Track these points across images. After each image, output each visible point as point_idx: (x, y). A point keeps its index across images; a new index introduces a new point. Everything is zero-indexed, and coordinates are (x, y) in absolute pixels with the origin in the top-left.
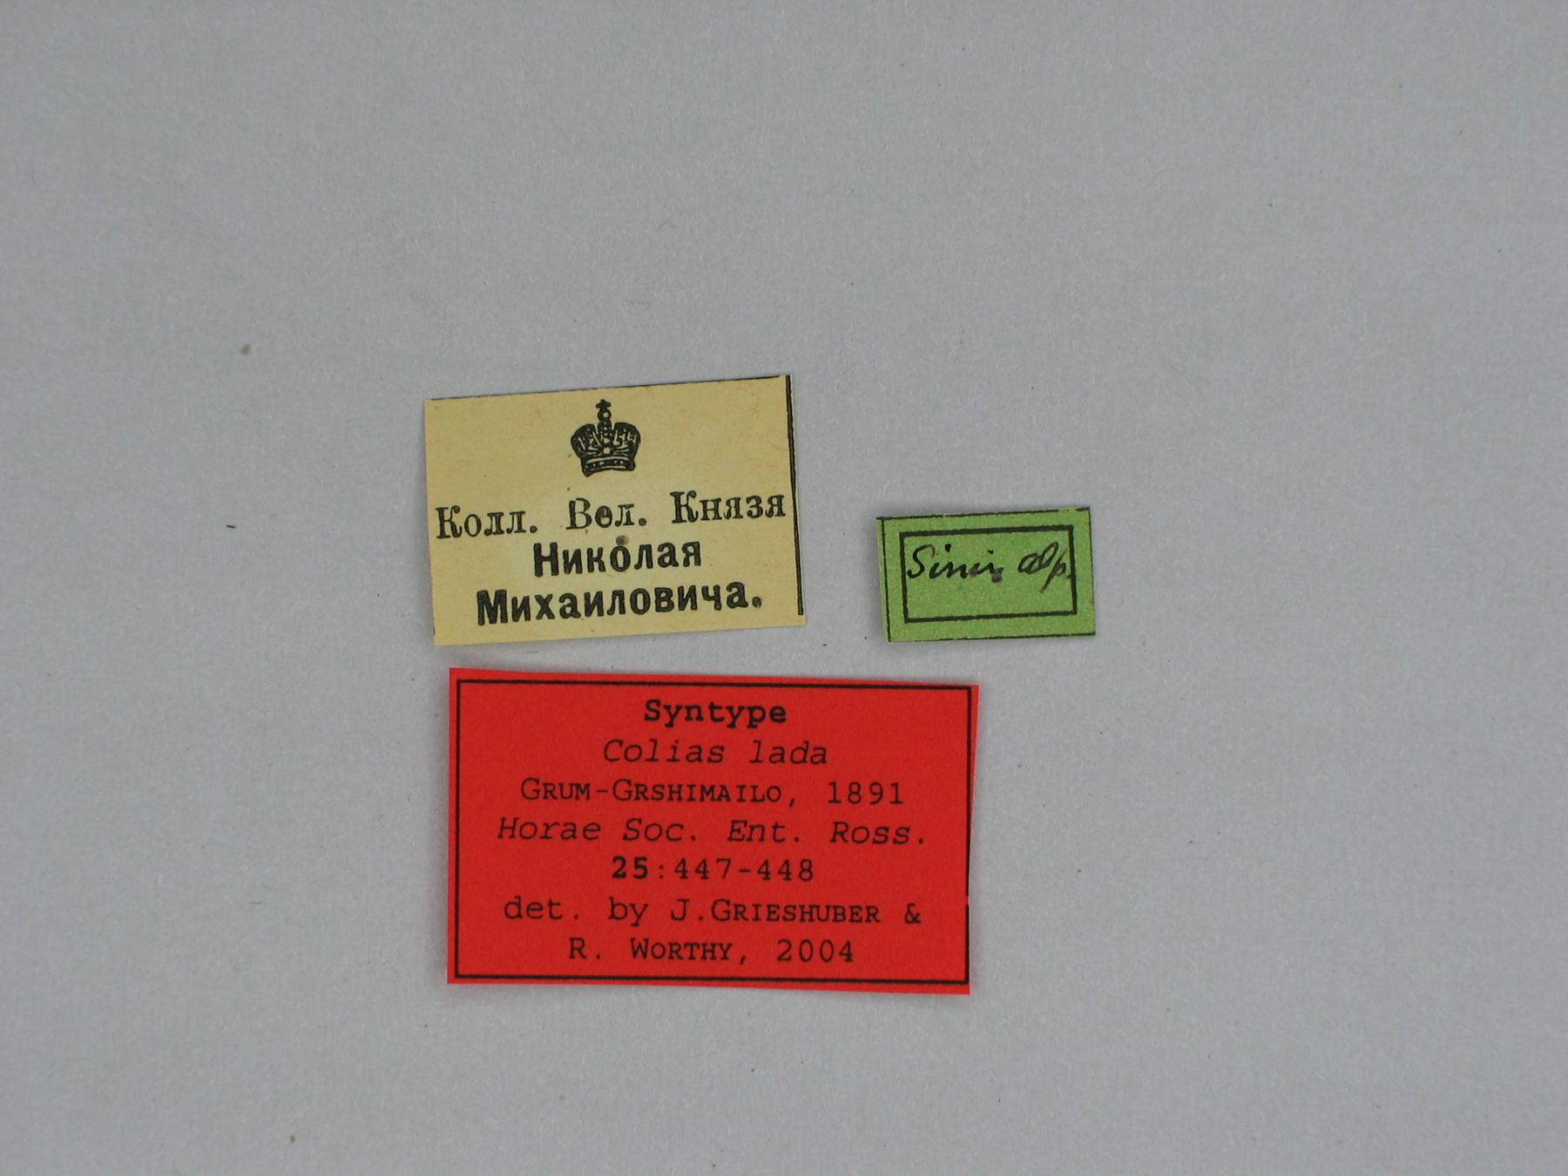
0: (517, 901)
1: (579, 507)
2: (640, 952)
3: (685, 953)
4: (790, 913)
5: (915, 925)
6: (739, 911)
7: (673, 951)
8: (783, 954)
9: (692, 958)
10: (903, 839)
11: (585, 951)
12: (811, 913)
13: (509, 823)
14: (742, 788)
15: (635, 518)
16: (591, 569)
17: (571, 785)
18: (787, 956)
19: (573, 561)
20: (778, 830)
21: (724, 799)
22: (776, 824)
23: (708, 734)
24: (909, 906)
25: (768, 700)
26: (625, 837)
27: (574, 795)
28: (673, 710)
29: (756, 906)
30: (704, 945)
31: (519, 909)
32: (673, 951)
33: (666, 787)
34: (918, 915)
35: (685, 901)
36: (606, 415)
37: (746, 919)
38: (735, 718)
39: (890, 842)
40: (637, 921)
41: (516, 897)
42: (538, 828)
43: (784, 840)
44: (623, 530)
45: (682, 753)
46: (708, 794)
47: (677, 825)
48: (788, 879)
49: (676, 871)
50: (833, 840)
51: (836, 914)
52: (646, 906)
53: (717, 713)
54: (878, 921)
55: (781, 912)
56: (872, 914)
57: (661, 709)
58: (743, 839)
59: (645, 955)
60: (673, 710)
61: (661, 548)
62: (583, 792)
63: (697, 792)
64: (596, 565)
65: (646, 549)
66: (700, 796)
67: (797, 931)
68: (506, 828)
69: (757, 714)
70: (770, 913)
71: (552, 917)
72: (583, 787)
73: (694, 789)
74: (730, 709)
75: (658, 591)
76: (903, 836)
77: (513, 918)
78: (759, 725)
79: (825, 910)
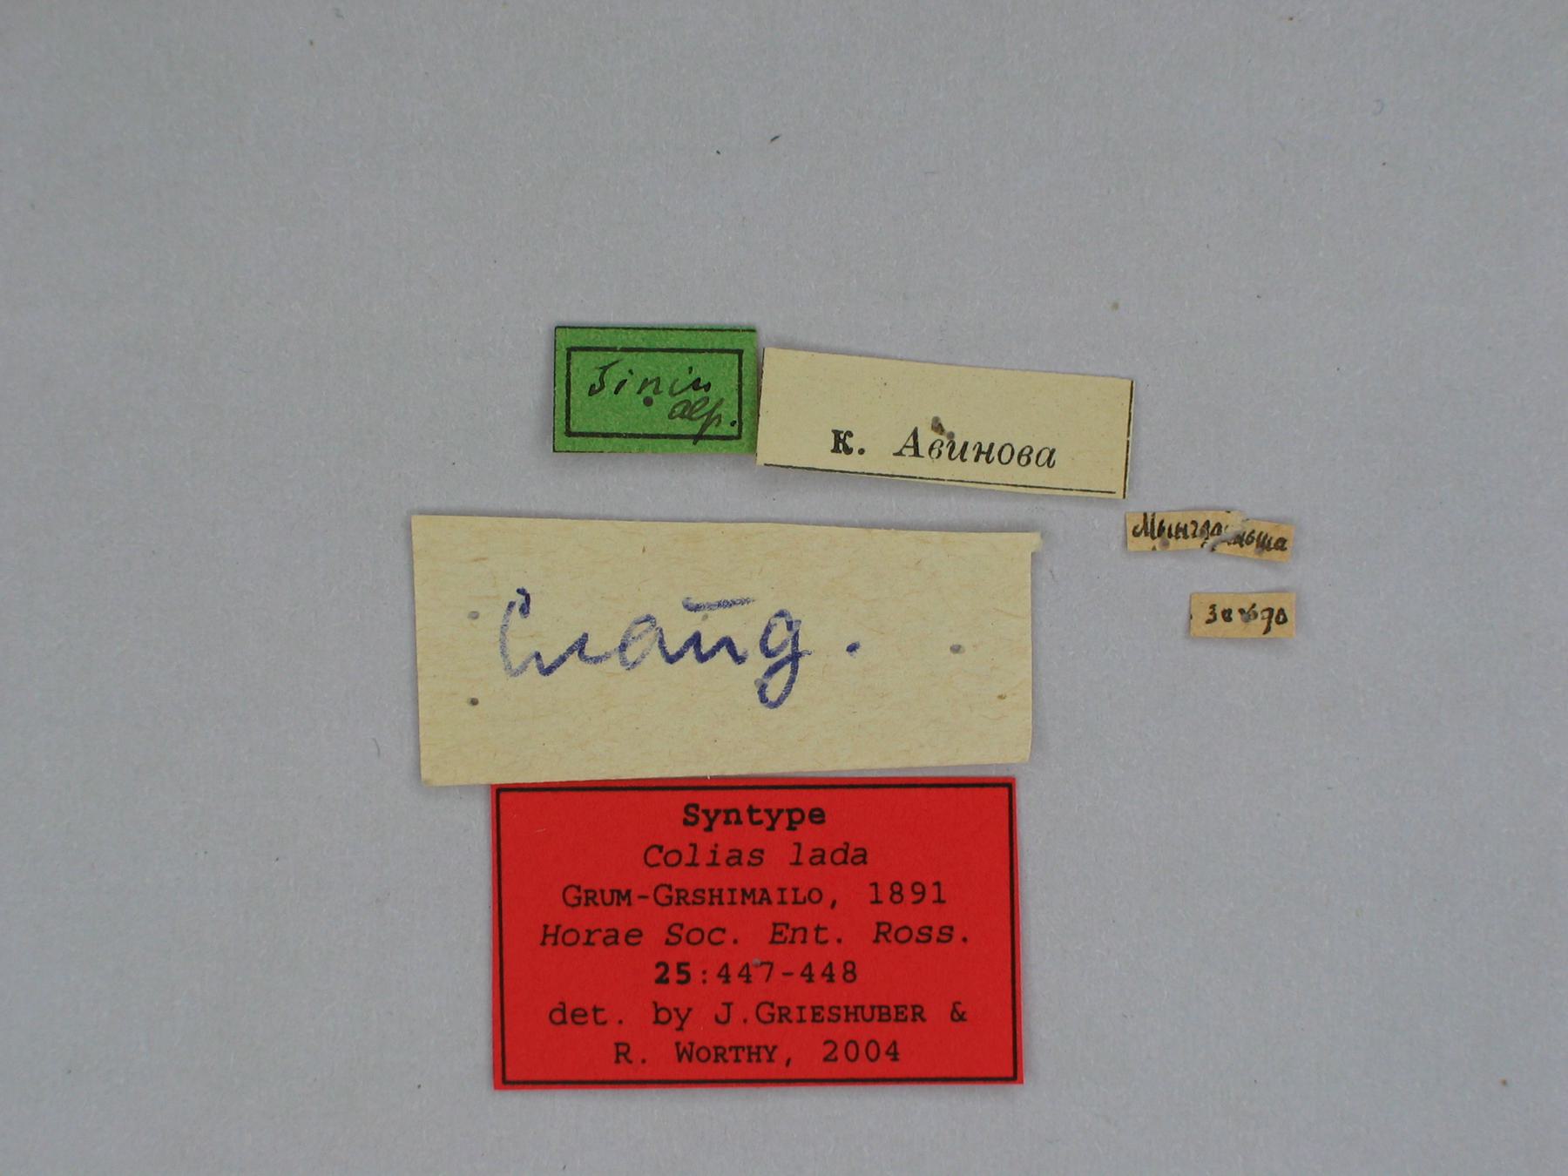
0: (561, 1007)
2: (685, 1055)
3: (730, 1055)
4: (833, 1014)
5: (961, 1022)
6: (784, 1015)
7: (719, 1054)
8: (830, 1055)
9: (737, 1060)
11: (630, 1056)
12: (856, 1014)
13: (551, 930)
14: (782, 890)
17: (612, 891)
18: (833, 1057)
20: (820, 932)
21: (765, 902)
23: (748, 837)
24: (954, 1004)
25: (806, 801)
26: (667, 942)
28: (712, 814)
29: (801, 1008)
31: (567, 1015)
32: (719, 1054)
34: (963, 1013)
37: (790, 1022)
38: (774, 821)
40: (682, 1024)
41: (561, 1003)
42: (581, 936)
43: (826, 942)
45: (722, 856)
46: (749, 898)
47: (718, 929)
48: (831, 980)
49: (719, 975)
50: (876, 941)
51: (881, 1014)
52: (689, 1010)
53: (756, 817)
54: (923, 1020)
55: (825, 1014)
56: (918, 1014)
57: (700, 814)
58: (784, 942)
59: (690, 1059)
60: (712, 814)
62: (624, 899)
63: (738, 897)
67: (842, 1031)
68: (550, 935)
69: (797, 816)
70: (814, 1014)
71: (597, 1023)
72: (624, 893)
73: (735, 893)
74: (769, 811)
77: (559, 1024)
78: (799, 827)
79: (870, 1010)
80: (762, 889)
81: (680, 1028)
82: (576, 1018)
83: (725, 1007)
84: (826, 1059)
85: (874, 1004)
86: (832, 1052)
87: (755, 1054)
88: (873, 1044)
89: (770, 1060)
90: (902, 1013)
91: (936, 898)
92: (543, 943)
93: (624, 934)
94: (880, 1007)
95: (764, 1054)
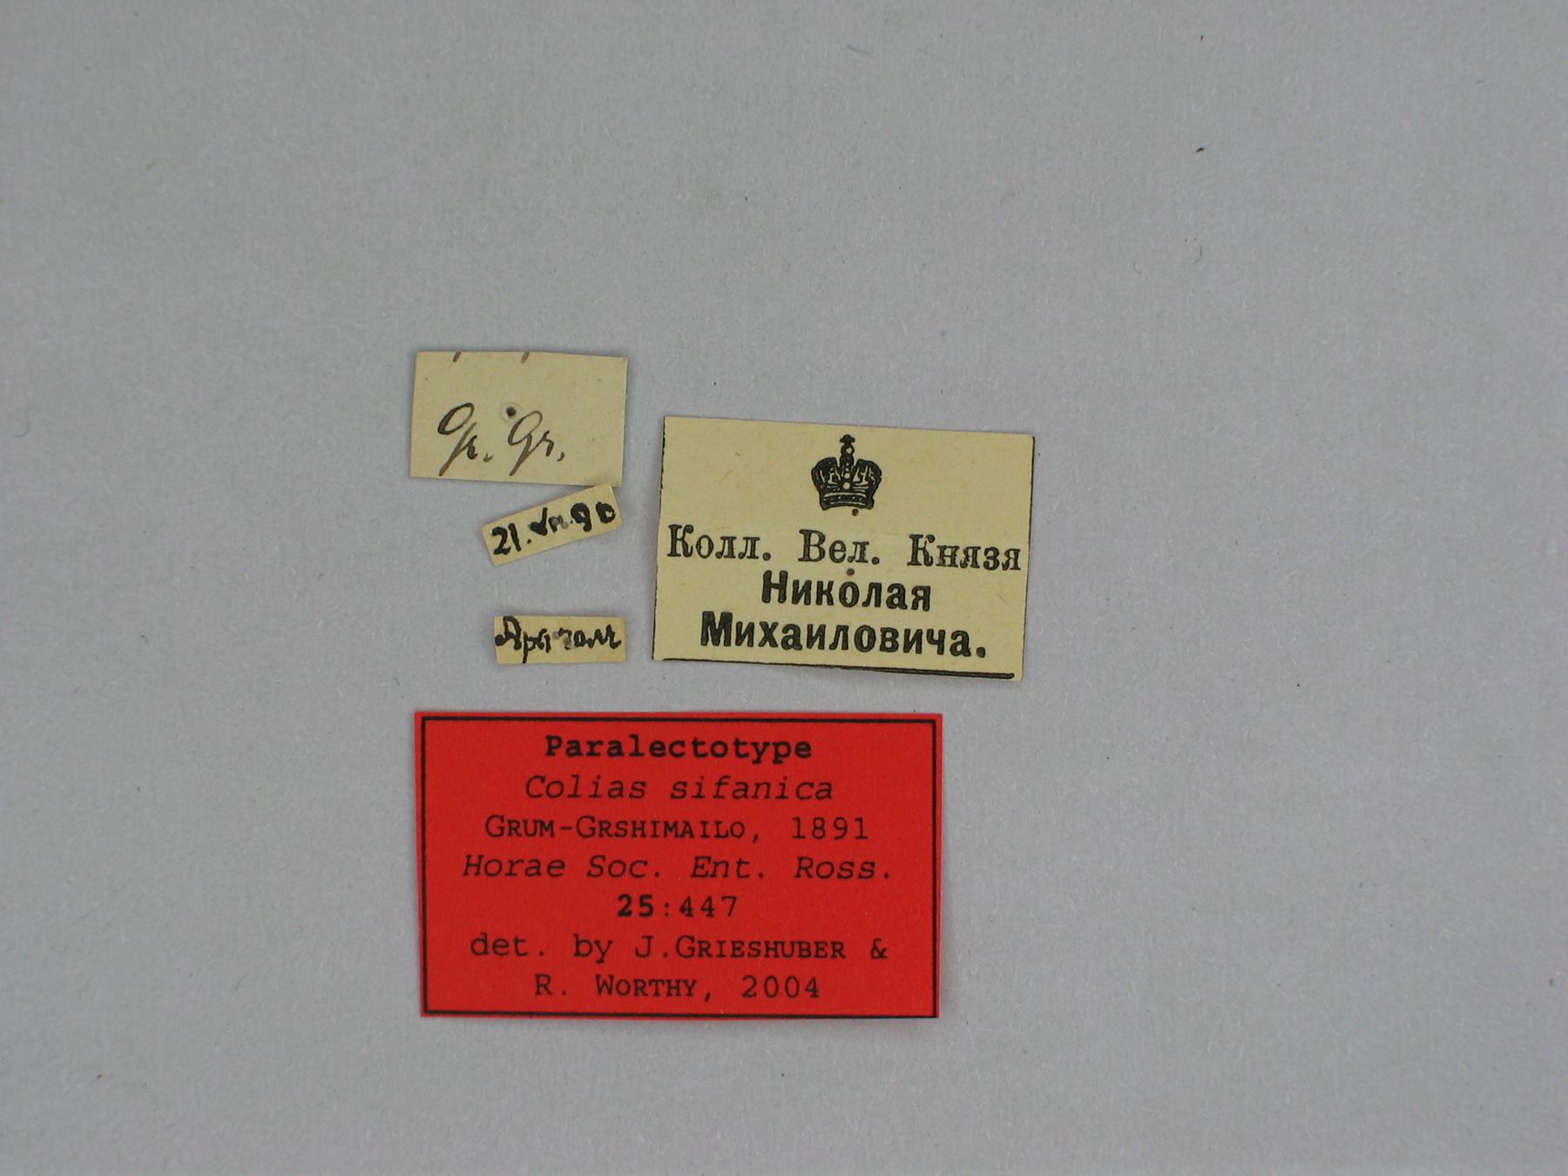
0: (482, 937)
1: (815, 539)
2: (605, 987)
5: (880, 959)
6: (704, 950)
7: (639, 988)
8: (749, 990)
9: (657, 994)
10: (869, 874)
11: (550, 988)
12: (775, 949)
13: (474, 860)
14: (704, 823)
15: (869, 556)
16: (819, 602)
19: (801, 595)
20: (743, 866)
21: (687, 835)
22: (740, 860)
24: (875, 941)
27: (538, 832)
29: (721, 943)
30: (669, 982)
31: (486, 946)
32: (639, 988)
33: (629, 823)
34: (884, 950)
35: (649, 938)
36: (849, 451)
37: (710, 955)
39: (855, 874)
40: (602, 958)
41: (482, 933)
42: (503, 867)
44: (855, 565)
46: (671, 830)
50: (798, 876)
51: (801, 949)
52: (610, 942)
55: (746, 949)
56: (838, 950)
59: (610, 992)
61: (890, 589)
62: (546, 830)
63: (661, 828)
64: (824, 597)
65: (875, 587)
66: (663, 828)
67: (761, 967)
70: (734, 949)
72: (547, 825)
73: (657, 825)
75: (884, 631)
76: (869, 870)
77: (481, 954)
80: (684, 822)
81: (601, 961)
82: (498, 950)
83: (646, 940)
84: (745, 995)
85: (795, 940)
86: (753, 987)
87: (673, 988)
88: (792, 981)
89: (690, 994)
90: (823, 949)
91: (858, 834)
92: (466, 874)
93: (546, 867)
94: (800, 943)
95: (683, 990)
